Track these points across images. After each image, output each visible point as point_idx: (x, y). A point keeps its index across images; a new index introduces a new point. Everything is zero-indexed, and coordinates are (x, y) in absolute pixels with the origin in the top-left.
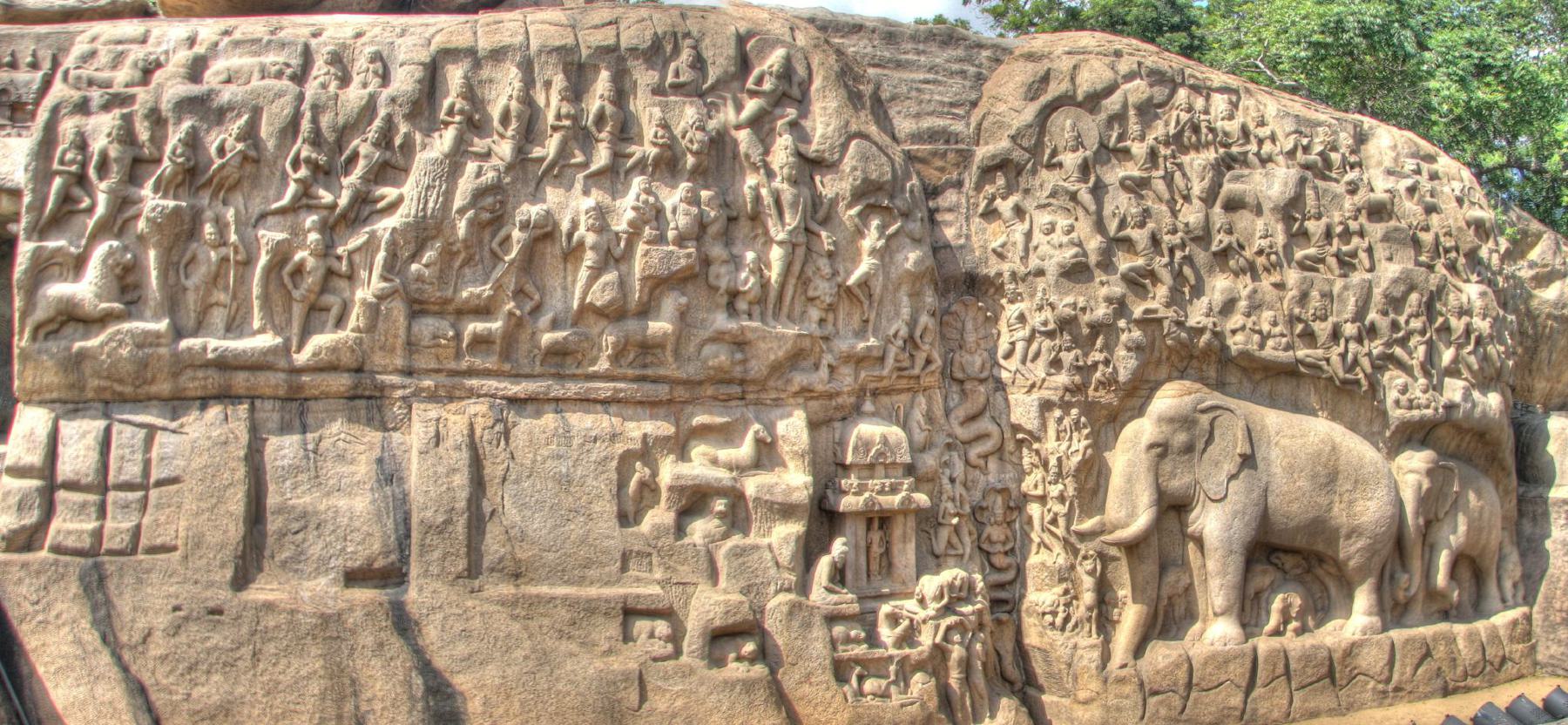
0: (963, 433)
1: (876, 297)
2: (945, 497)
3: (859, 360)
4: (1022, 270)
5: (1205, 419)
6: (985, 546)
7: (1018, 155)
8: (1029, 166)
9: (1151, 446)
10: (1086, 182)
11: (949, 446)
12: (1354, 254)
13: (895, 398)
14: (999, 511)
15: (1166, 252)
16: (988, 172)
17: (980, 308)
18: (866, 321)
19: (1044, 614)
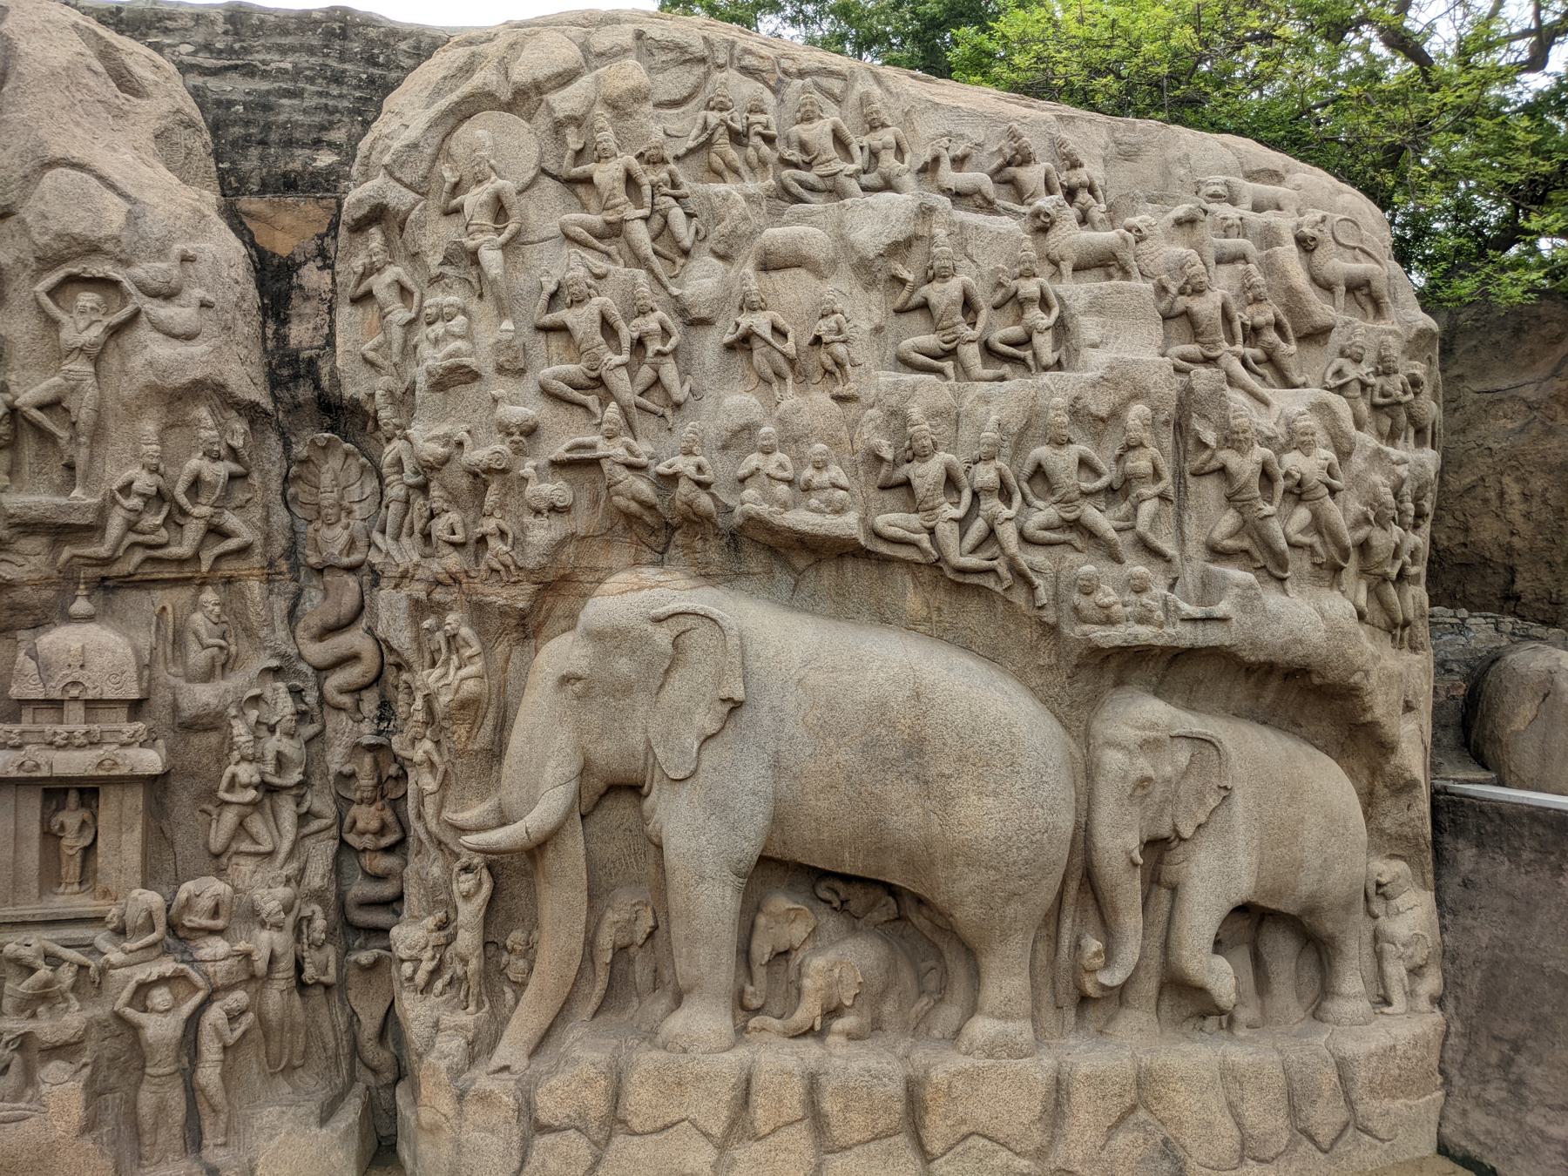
0: (318, 652)
1: (81, 426)
2: (236, 755)
3: (59, 532)
4: (400, 388)
5: (662, 637)
6: (351, 838)
7: (399, 198)
8: (416, 212)
9: (566, 680)
10: (499, 232)
11: (276, 672)
12: (1026, 342)
13: (159, 593)
14: (366, 781)
15: (626, 345)
16: (360, 227)
17: (347, 454)
18: (70, 467)
19: (403, 961)
